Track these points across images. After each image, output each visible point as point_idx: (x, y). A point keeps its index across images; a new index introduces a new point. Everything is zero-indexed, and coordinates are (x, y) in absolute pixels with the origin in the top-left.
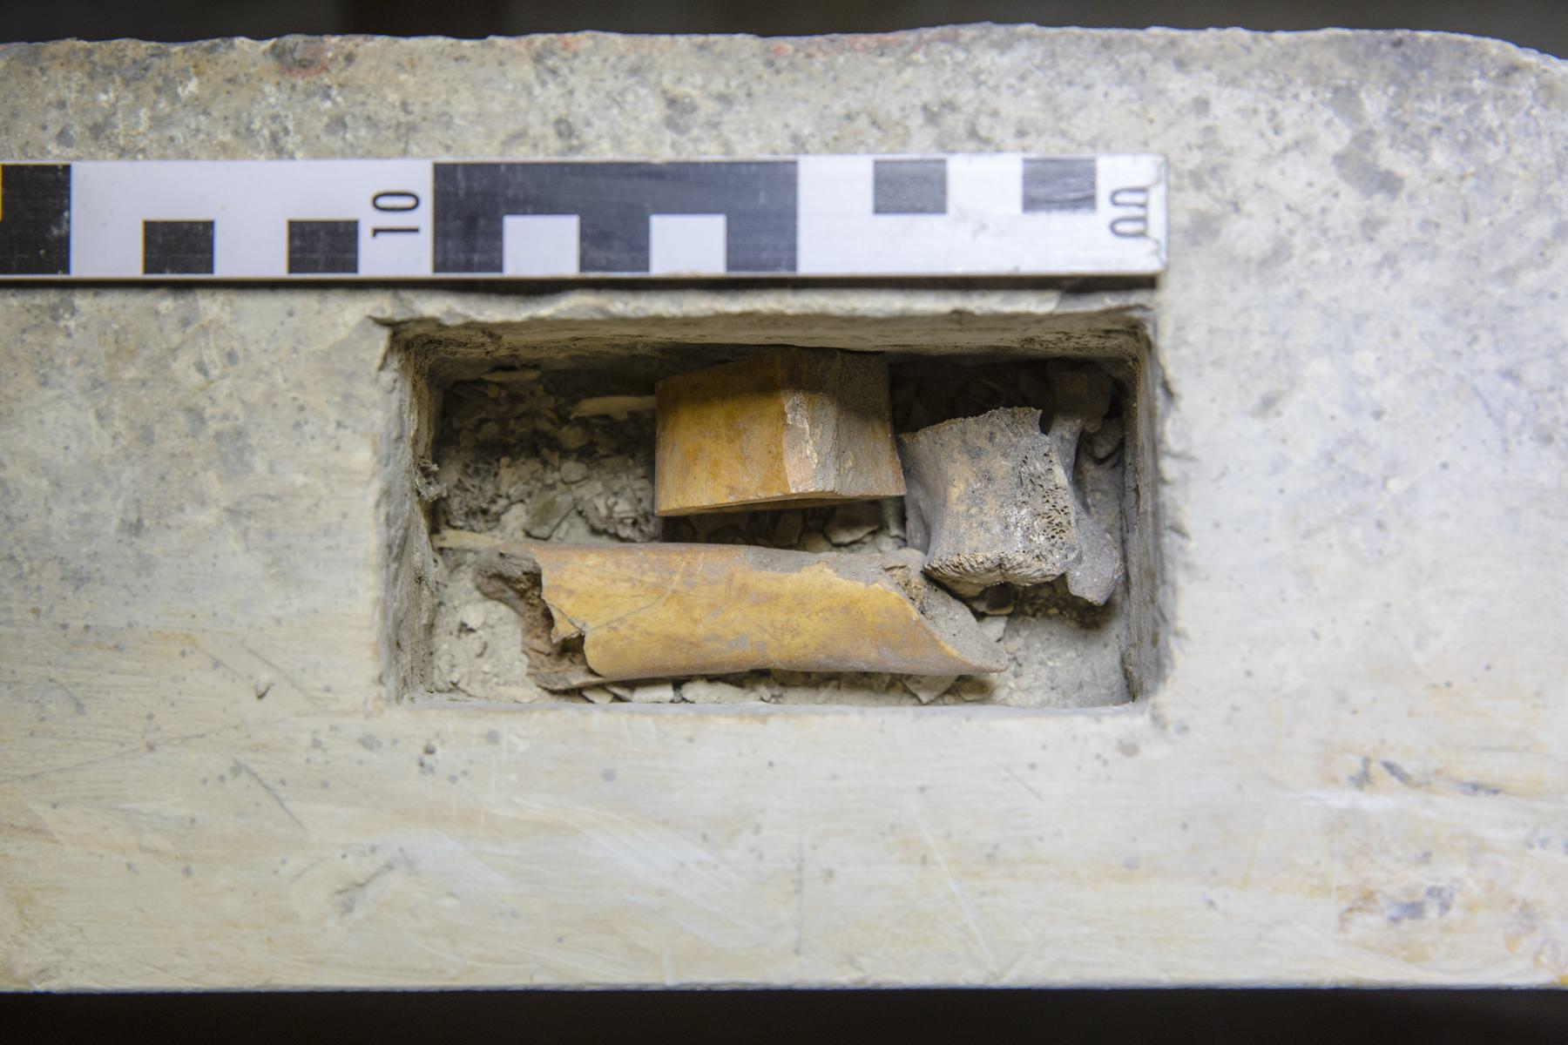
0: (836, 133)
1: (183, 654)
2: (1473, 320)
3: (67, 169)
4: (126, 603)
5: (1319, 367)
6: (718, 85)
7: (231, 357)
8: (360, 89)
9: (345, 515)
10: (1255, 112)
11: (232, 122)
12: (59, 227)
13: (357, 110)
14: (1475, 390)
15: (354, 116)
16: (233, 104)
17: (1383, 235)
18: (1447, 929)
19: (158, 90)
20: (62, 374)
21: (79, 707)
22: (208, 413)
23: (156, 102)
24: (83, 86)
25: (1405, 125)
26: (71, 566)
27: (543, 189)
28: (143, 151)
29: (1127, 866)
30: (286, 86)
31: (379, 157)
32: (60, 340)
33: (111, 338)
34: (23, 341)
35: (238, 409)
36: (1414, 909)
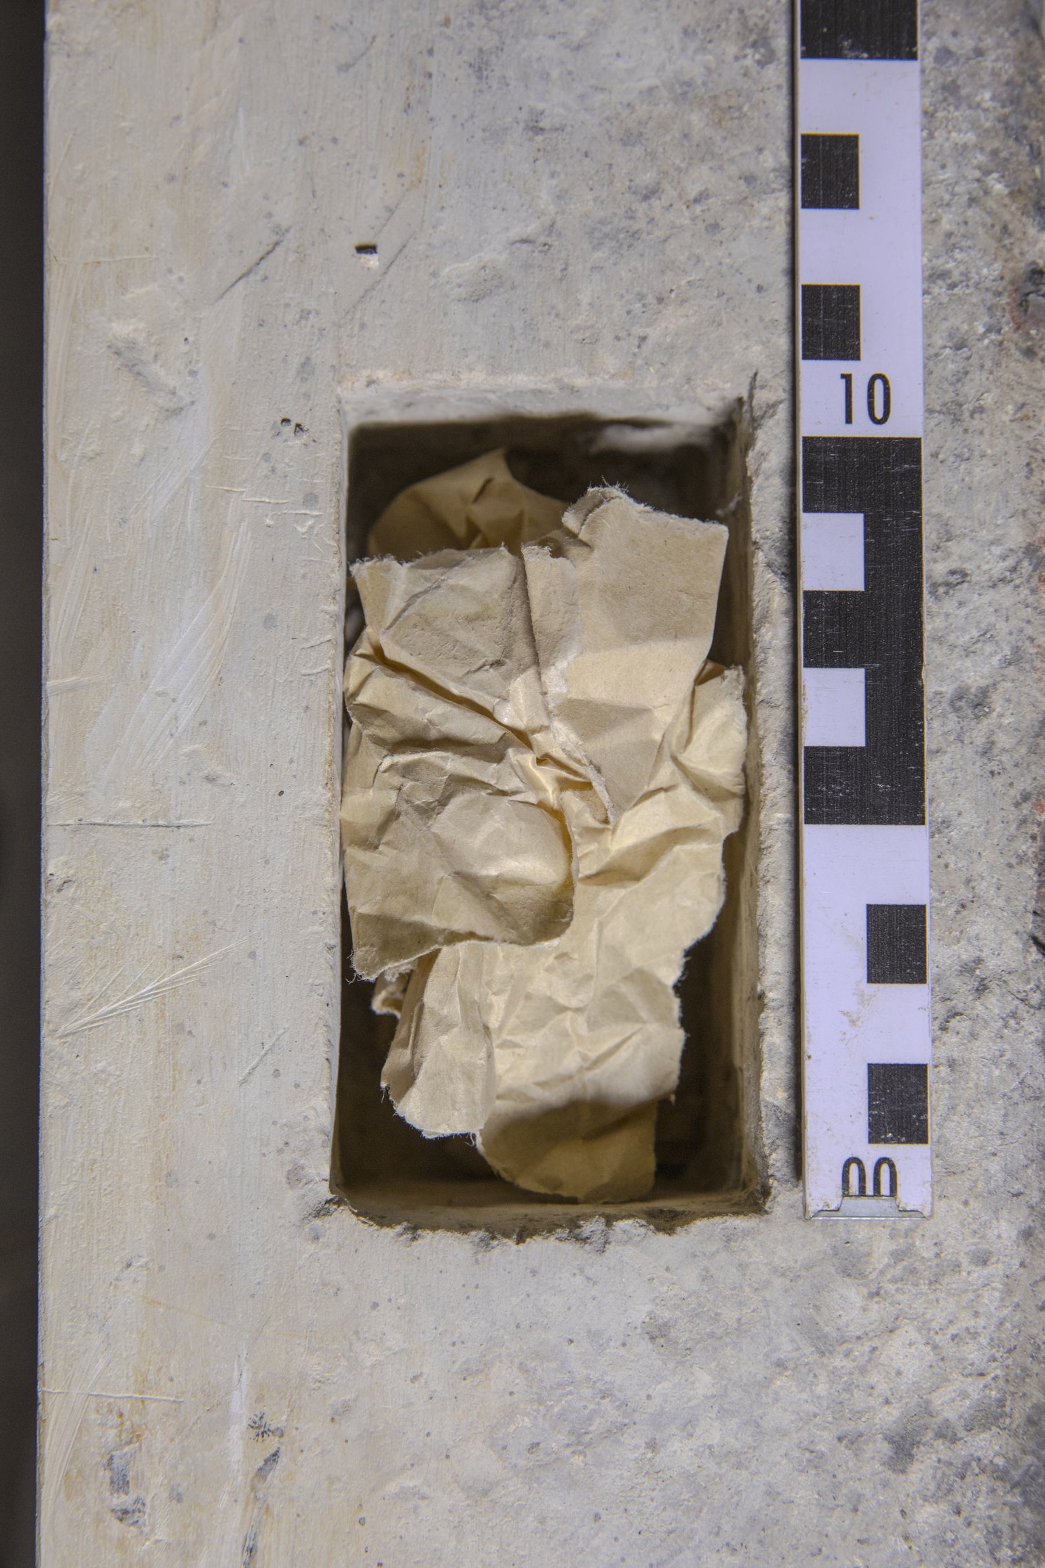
0: (952, 866)
1: (401, 175)
2: (753, 1545)
3: (913, 56)
4: (454, 117)
5: (704, 1382)
6: (1004, 740)
7: (714, 227)
8: (998, 364)
9: (547, 345)
10: (976, 1314)
11: (963, 229)
12: (852, 48)
13: (975, 360)
14: (680, 1551)
15: (968, 358)
16: (981, 231)
17: (844, 1452)
19: (995, 153)
20: (696, 52)
21: (346, 67)
22: (655, 202)
23: (982, 149)
24: (1000, 75)
25: (963, 1478)
26: (493, 59)
27: (896, 551)
28: (931, 136)
29: (169, 1175)
30: (1000, 286)
31: (926, 384)
32: (732, 50)
33: (733, 102)
34: (730, 11)
35: (659, 233)
36: (121, 1483)
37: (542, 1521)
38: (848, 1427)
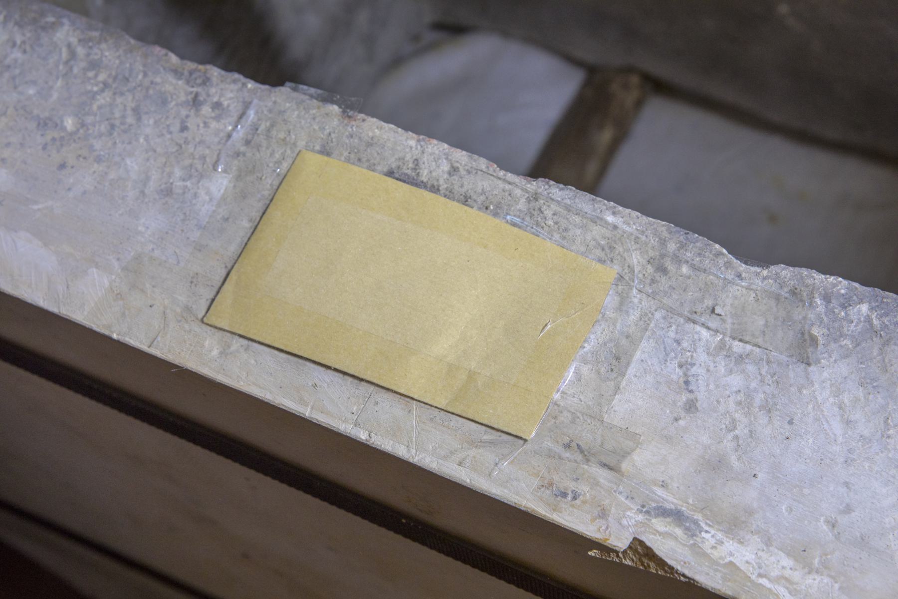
18: (572, 506)
36: (564, 495)
37: (636, 376)
38: (648, 281)
